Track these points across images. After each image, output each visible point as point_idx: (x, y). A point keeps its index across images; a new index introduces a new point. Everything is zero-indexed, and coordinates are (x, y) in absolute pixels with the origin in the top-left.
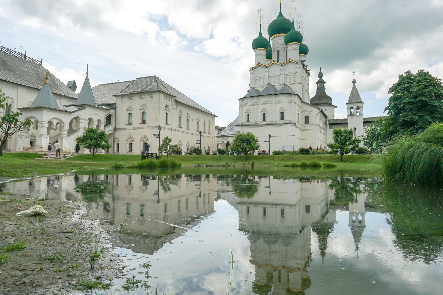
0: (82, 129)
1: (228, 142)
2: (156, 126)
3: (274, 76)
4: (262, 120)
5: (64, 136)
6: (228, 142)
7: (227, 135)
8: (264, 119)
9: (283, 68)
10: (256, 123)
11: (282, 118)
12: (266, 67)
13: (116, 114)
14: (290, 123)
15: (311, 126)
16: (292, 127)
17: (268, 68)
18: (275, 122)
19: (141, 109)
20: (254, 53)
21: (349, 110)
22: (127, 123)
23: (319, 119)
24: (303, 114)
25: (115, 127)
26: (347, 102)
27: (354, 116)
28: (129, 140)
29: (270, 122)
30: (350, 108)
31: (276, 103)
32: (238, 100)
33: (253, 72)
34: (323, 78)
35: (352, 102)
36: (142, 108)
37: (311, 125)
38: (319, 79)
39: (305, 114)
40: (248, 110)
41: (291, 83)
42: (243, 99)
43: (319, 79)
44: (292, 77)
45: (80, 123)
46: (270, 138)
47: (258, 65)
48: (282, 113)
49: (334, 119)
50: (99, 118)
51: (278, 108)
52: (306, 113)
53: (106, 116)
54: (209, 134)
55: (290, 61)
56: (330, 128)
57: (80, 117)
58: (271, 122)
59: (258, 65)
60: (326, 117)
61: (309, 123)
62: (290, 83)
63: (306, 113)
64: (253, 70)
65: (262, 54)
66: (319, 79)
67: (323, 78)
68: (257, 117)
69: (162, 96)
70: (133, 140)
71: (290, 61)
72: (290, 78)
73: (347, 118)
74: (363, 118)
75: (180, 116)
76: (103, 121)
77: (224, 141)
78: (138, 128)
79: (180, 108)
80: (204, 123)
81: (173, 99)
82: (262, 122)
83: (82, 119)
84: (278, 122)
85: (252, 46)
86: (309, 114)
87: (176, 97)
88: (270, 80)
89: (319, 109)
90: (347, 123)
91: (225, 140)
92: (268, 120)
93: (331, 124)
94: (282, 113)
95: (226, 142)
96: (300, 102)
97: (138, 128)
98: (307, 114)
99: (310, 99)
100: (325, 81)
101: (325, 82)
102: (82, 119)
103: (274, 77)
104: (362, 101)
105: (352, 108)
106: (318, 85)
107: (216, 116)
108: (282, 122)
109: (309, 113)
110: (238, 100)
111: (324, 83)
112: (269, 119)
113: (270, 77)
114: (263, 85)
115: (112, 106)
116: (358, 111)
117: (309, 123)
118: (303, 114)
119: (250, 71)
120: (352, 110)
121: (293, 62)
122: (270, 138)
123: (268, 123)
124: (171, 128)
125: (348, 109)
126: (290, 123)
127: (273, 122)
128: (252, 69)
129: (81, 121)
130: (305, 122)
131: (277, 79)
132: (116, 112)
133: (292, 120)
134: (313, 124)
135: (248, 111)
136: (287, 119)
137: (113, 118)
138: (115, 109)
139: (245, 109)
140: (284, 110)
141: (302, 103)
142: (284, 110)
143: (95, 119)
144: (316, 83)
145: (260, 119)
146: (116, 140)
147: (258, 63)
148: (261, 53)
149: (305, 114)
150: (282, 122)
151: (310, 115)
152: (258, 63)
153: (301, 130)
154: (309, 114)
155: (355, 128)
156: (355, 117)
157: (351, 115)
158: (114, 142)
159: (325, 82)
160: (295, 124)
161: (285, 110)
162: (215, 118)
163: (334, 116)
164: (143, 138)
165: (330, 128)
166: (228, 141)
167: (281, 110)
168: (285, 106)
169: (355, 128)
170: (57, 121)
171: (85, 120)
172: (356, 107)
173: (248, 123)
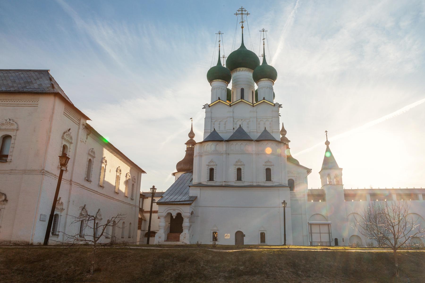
1: (179, 215)
4: (236, 180)
6: (179, 215)
7: (176, 200)
8: (239, 178)
9: (255, 108)
18: (257, 184)
33: (209, 109)
40: (211, 161)
48: (268, 171)
54: (132, 199)
55: (265, 101)
71: (265, 101)
72: (265, 124)
77: (171, 211)
82: (235, 183)
84: (262, 184)
91: (174, 210)
94: (268, 171)
95: (174, 215)
100: (289, 139)
103: (240, 120)
107: (144, 172)
113: (236, 120)
119: (205, 109)
123: (246, 184)
135: (212, 164)
140: (272, 165)
142: (272, 165)
145: (232, 178)
159: (289, 141)
161: (273, 165)
166: (179, 212)
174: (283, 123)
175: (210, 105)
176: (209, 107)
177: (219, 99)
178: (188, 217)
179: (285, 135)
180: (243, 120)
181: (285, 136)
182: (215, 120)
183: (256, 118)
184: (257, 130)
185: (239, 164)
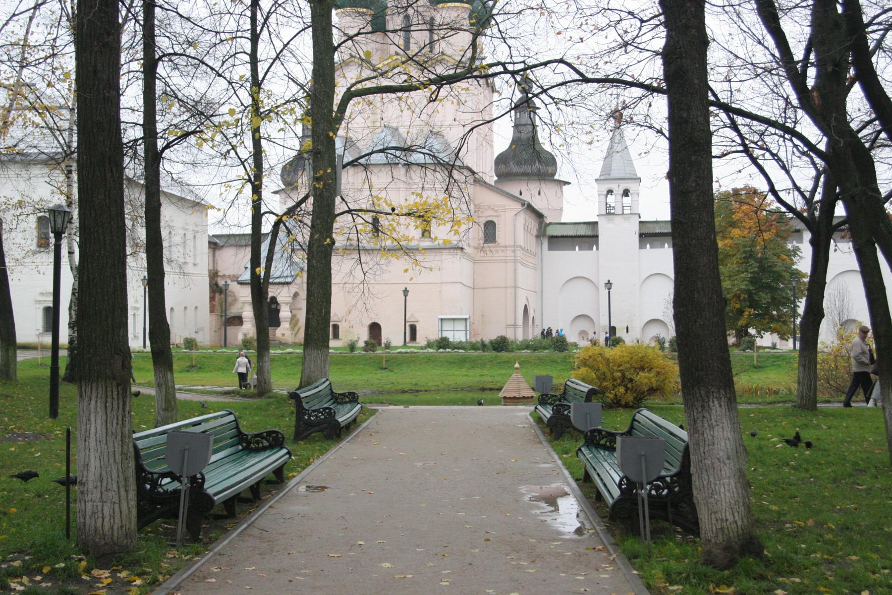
15: (503, 251)
21: (605, 197)
23: (522, 229)
26: (597, 177)
27: (616, 217)
30: (605, 193)
35: (612, 176)
46: (406, 296)
49: (563, 221)
56: (550, 249)
60: (539, 216)
73: (595, 219)
74: (641, 222)
80: (184, 232)
86: (497, 216)
89: (523, 205)
90: (597, 236)
93: (552, 238)
98: (488, 215)
99: (495, 156)
104: (639, 176)
105: (610, 192)
106: (518, 116)
108: (426, 243)
109: (495, 214)
116: (627, 200)
120: (611, 199)
122: (406, 296)
125: (599, 195)
134: (506, 247)
150: (426, 243)
151: (499, 219)
153: (475, 262)
154: (497, 216)
155: (609, 281)
156: (618, 220)
157: (609, 212)
160: (462, 249)
163: (561, 210)
165: (550, 249)
169: (609, 281)
172: (622, 192)
178: (287, 304)
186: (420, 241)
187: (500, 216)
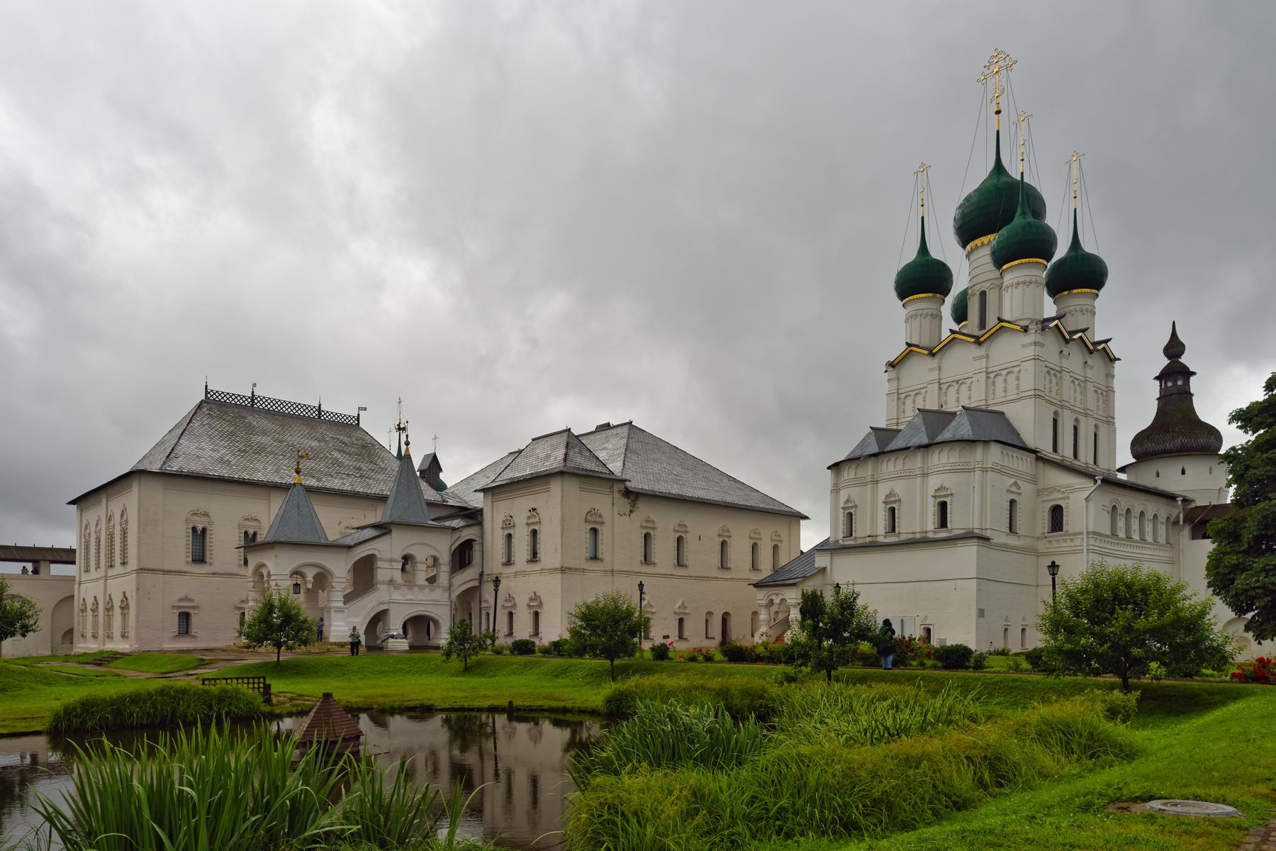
0: (383, 583)
2: (556, 569)
3: (957, 382)
5: (334, 604)
10: (868, 540)
11: (943, 523)
12: (932, 355)
13: (482, 537)
14: (968, 536)
16: (968, 554)
17: (938, 356)
18: (924, 535)
19: (528, 524)
20: (903, 313)
22: (504, 560)
24: (1045, 499)
25: (480, 570)
28: (507, 605)
29: (910, 536)
31: (925, 475)
32: (829, 468)
34: (1184, 360)
36: (531, 521)
37: (1069, 535)
38: (1166, 362)
39: (1052, 500)
41: (1008, 398)
42: (841, 465)
43: (1169, 362)
44: (1012, 378)
45: (379, 570)
47: (911, 350)
48: (943, 507)
50: (435, 553)
51: (882, 498)
52: (1052, 496)
53: (452, 545)
57: (378, 556)
58: (913, 536)
59: (908, 351)
61: (1062, 530)
62: (1004, 399)
63: (1052, 496)
64: (896, 368)
65: (925, 312)
66: (1166, 362)
67: (1183, 360)
68: (872, 524)
69: (573, 487)
70: (541, 604)
75: (645, 531)
76: (445, 558)
78: (524, 573)
79: (645, 510)
81: (617, 487)
83: (382, 560)
85: (897, 289)
86: (1063, 498)
87: (625, 481)
88: (946, 393)
92: (902, 531)
94: (943, 507)
96: (1033, 461)
97: (524, 573)
98: (1055, 498)
101: (1194, 373)
102: (382, 560)
109: (1063, 496)
110: (829, 468)
111: (1187, 374)
112: (909, 526)
113: (944, 387)
114: (1016, 391)
115: (473, 516)
117: (1062, 530)
118: (1046, 501)
121: (1010, 326)
123: (903, 537)
124: (610, 570)
126: (968, 536)
127: (918, 536)
128: (892, 365)
129: (379, 564)
130: (1053, 524)
131: (964, 388)
132: (482, 533)
133: (976, 526)
134: (1075, 534)
136: (957, 523)
137: (476, 547)
138: (480, 524)
139: (843, 496)
140: (946, 496)
141: (1041, 464)
142: (946, 496)
143: (421, 554)
144: (1157, 378)
146: (484, 605)
147: (907, 343)
148: (920, 312)
149: (1052, 500)
150: (943, 534)
152: (907, 343)
154: (1063, 498)
158: (481, 611)
159: (1194, 373)
161: (952, 495)
162: (801, 521)
164: (531, 600)
167: (940, 496)
168: (949, 481)
170: (316, 571)
171: (391, 560)
173: (850, 542)
174: (1174, 322)
175: (895, 363)
176: (893, 367)
177: (909, 345)
179: (1180, 358)
180: (960, 382)
181: (1180, 360)
182: (906, 394)
183: (984, 373)
184: (986, 400)
185: (893, 499)
186: (935, 533)
187: (1068, 498)
